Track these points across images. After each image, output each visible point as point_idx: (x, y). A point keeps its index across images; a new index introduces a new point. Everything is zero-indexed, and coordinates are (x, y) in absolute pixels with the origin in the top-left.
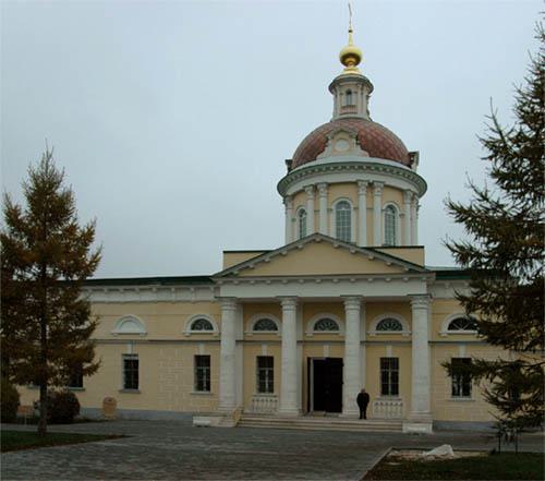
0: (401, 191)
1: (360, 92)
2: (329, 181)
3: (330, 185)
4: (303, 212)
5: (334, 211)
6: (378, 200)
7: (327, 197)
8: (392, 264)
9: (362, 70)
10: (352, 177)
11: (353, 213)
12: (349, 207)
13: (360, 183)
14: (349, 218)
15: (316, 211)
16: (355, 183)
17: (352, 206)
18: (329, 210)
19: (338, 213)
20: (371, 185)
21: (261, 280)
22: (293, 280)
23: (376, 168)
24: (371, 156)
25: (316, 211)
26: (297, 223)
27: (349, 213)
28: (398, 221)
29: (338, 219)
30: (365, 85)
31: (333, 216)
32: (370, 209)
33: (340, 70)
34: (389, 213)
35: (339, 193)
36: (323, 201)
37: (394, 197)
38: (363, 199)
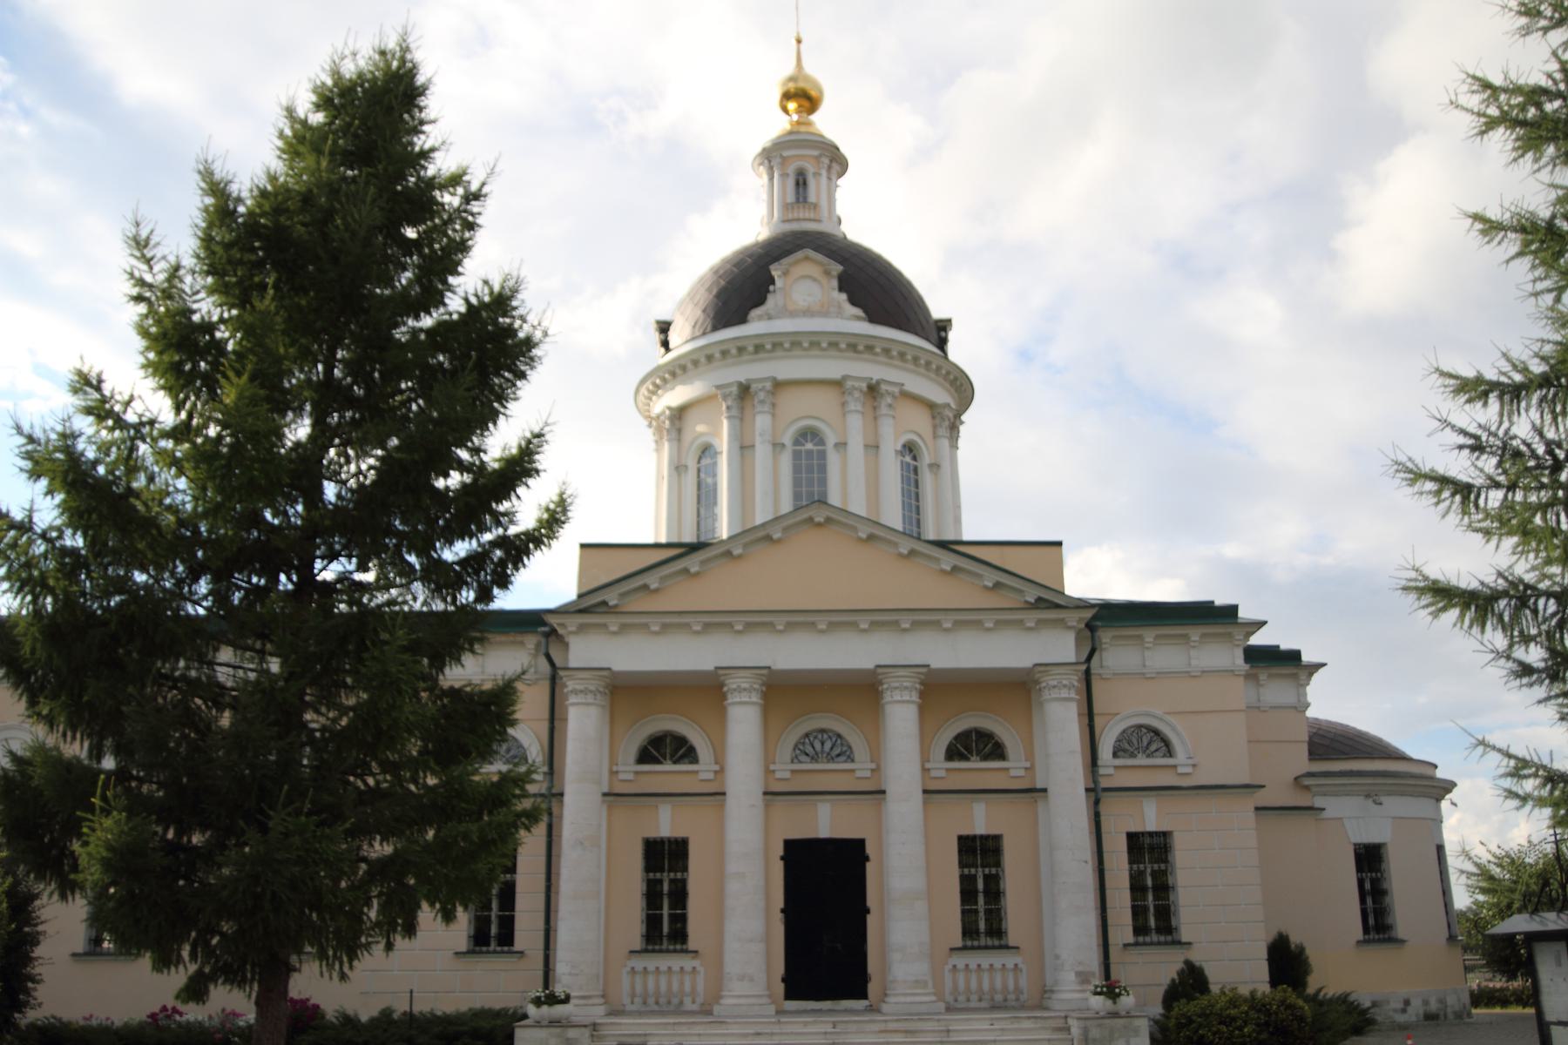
0: (931, 406)
1: (824, 172)
2: (781, 376)
3: (778, 385)
4: (707, 450)
7: (773, 415)
8: (998, 585)
9: (824, 122)
10: (832, 368)
11: (833, 459)
12: (822, 442)
13: (849, 384)
14: (823, 469)
16: (838, 384)
17: (831, 439)
18: (777, 446)
19: (797, 455)
20: (873, 390)
21: (675, 623)
22: (758, 621)
23: (885, 351)
24: (873, 318)
26: (690, 479)
27: (822, 455)
28: (927, 479)
29: (797, 469)
30: (836, 161)
31: (786, 461)
32: (873, 447)
33: (777, 123)
34: (908, 459)
35: (802, 408)
36: (762, 422)
37: (917, 423)
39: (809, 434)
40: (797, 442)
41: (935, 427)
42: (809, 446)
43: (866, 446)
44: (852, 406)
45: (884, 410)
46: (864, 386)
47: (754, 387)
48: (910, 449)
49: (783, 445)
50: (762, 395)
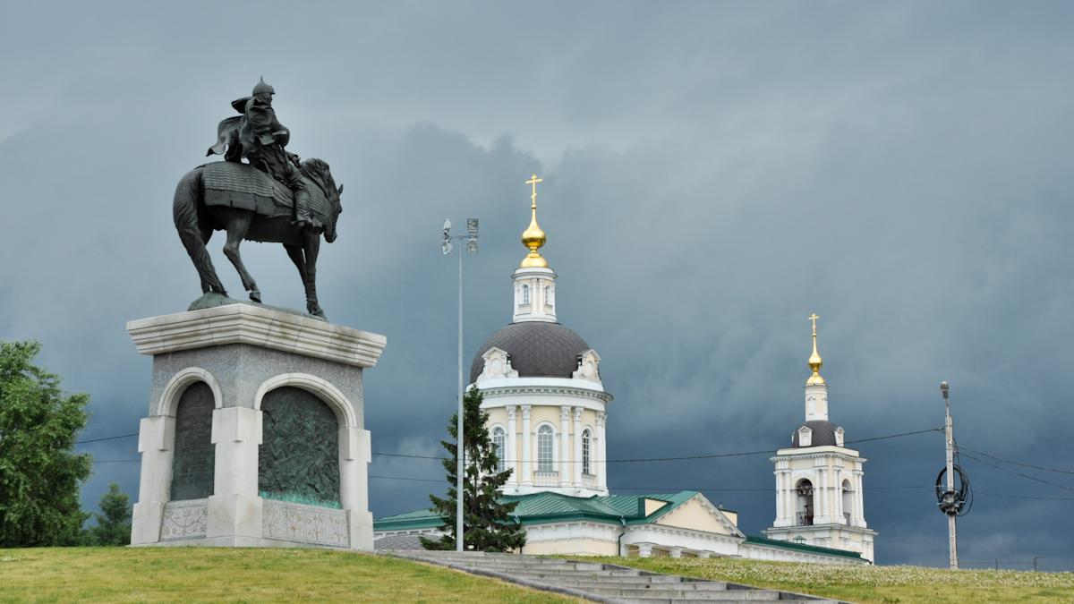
0: (595, 411)
3: (533, 406)
5: (537, 434)
6: (578, 425)
7: (531, 419)
11: (555, 441)
12: (551, 431)
13: (563, 408)
14: (551, 443)
15: (519, 434)
17: (555, 431)
18: (533, 434)
19: (540, 437)
20: (573, 408)
25: (519, 434)
27: (551, 437)
29: (540, 443)
31: (536, 439)
34: (585, 436)
36: (527, 423)
38: (566, 425)
39: (545, 428)
40: (540, 431)
41: (596, 421)
42: (545, 433)
43: (570, 435)
44: (564, 417)
45: (577, 418)
46: (570, 409)
47: (522, 408)
48: (586, 432)
49: (534, 434)
50: (526, 412)
